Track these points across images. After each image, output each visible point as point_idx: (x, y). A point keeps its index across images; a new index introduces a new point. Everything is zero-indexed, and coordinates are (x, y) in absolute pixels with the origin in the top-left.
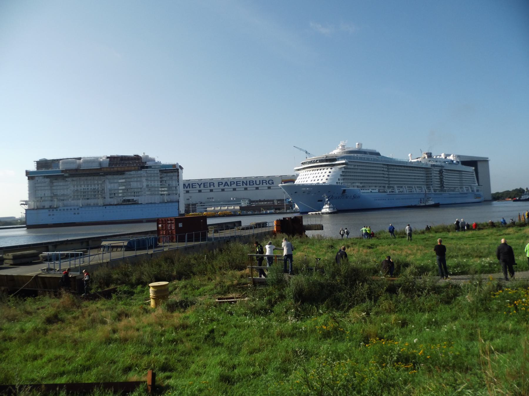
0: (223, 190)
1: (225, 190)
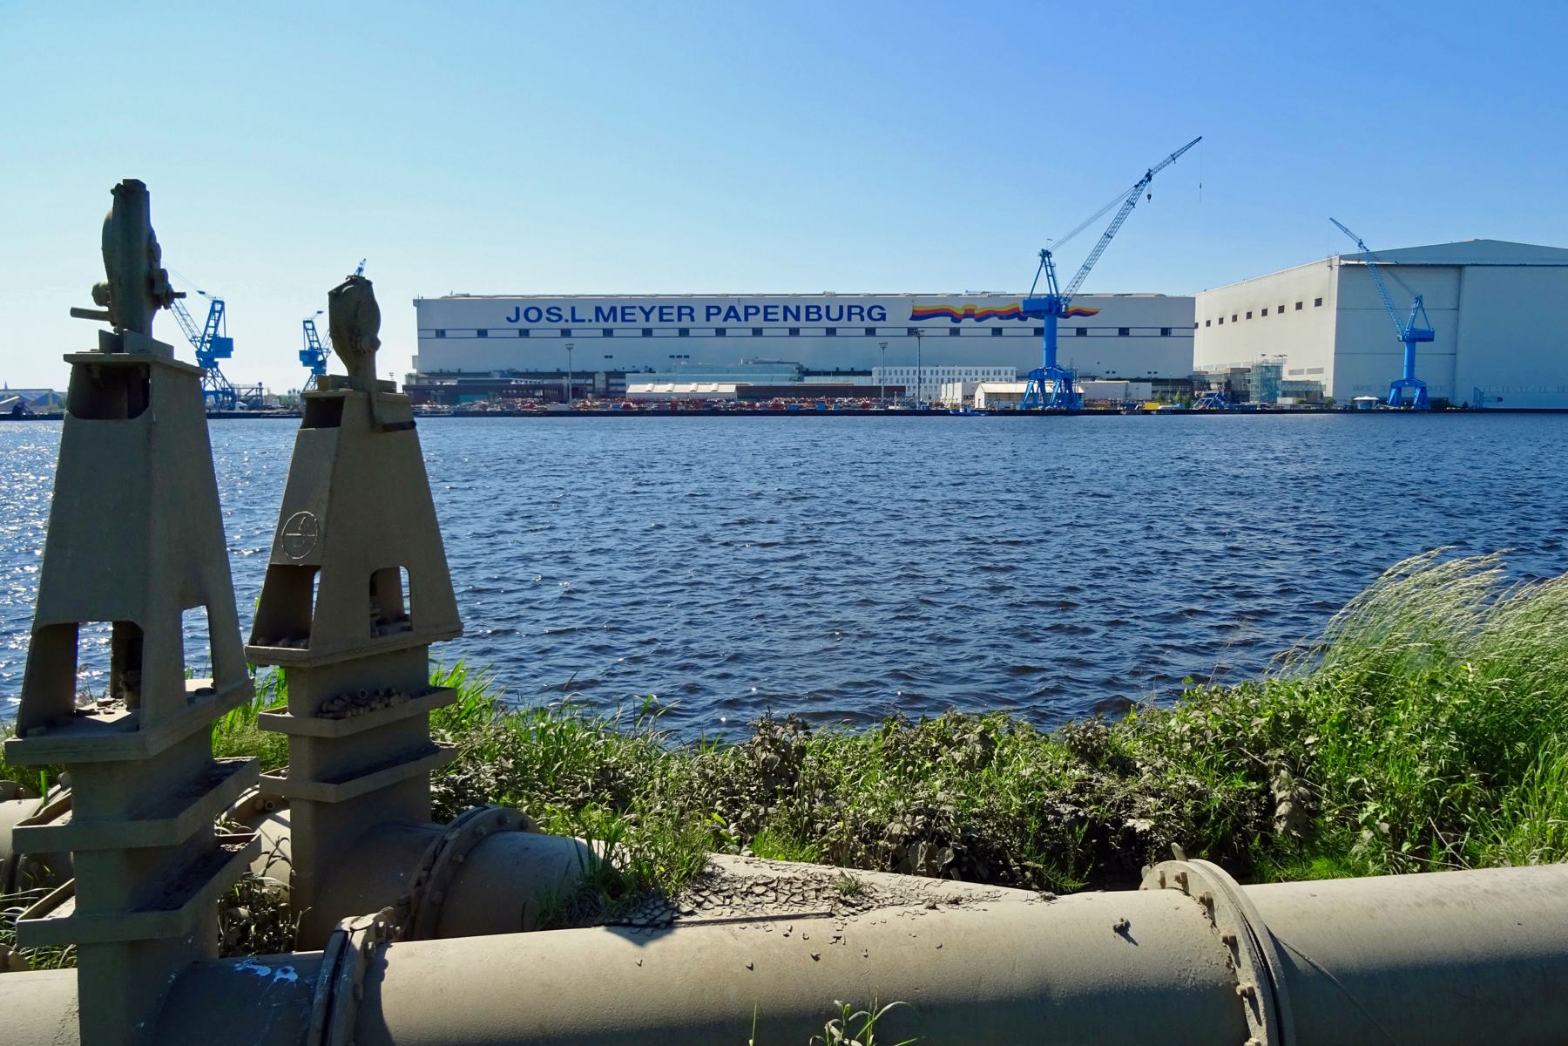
0: (721, 332)
1: (728, 332)
